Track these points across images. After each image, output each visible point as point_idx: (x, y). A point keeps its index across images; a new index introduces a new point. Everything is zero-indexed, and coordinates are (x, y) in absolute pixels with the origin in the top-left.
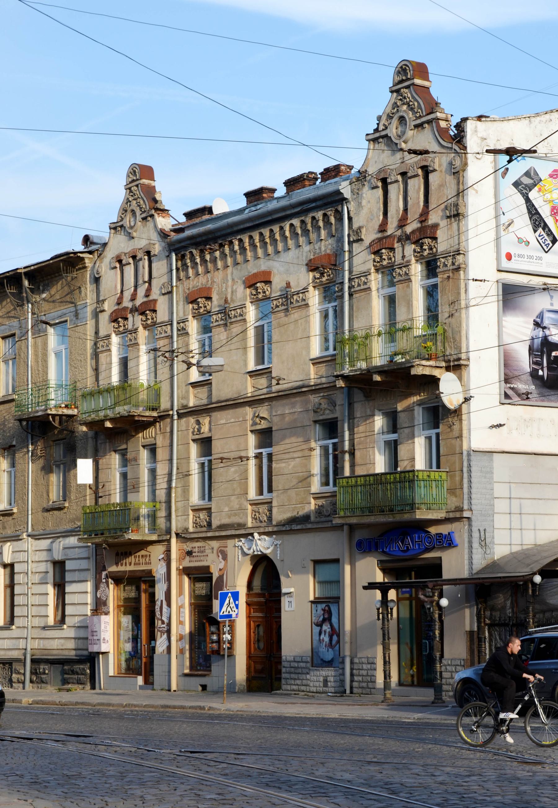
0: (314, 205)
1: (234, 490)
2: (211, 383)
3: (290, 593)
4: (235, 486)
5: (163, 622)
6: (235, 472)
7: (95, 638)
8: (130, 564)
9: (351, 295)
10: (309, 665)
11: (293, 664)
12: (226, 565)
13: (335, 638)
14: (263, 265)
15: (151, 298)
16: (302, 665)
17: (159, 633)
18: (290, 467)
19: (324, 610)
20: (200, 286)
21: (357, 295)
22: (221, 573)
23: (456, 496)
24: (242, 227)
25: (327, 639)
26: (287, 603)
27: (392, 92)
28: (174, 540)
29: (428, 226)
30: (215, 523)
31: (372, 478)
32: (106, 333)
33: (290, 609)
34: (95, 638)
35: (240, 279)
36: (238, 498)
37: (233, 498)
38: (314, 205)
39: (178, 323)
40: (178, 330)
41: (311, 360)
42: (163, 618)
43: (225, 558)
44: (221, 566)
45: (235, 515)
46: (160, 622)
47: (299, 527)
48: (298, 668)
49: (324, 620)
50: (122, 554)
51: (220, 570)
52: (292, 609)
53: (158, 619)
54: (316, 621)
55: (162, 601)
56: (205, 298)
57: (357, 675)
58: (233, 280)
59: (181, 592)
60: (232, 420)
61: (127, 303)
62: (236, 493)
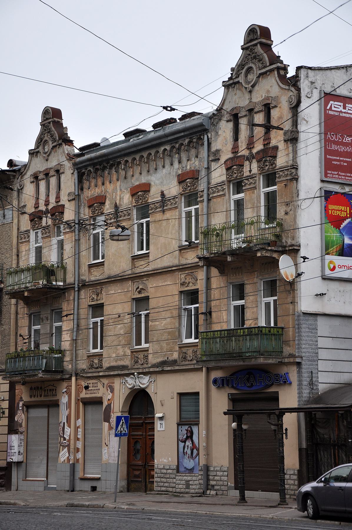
0: (183, 134)
5: (65, 439)
6: (121, 329)
7: (13, 451)
8: (41, 396)
13: (195, 451)
14: (144, 179)
15: (60, 204)
17: (61, 447)
18: (162, 325)
19: (187, 430)
20: (96, 195)
21: (215, 200)
22: (109, 402)
23: (290, 346)
24: (128, 151)
25: (189, 452)
26: (159, 425)
27: (243, 49)
28: (74, 379)
29: (270, 148)
31: (226, 332)
32: (25, 229)
33: (161, 429)
34: (13, 451)
35: (126, 189)
36: (123, 347)
37: (119, 347)
38: (183, 134)
42: (65, 436)
43: (112, 391)
44: (110, 397)
45: (121, 360)
46: (62, 439)
47: (169, 368)
48: (166, 473)
49: (187, 438)
50: (35, 389)
51: (109, 400)
52: (163, 429)
53: (61, 437)
54: (181, 439)
55: (64, 423)
56: (99, 203)
58: (121, 190)
59: (77, 417)
60: (119, 291)
61: (42, 208)
62: (121, 343)
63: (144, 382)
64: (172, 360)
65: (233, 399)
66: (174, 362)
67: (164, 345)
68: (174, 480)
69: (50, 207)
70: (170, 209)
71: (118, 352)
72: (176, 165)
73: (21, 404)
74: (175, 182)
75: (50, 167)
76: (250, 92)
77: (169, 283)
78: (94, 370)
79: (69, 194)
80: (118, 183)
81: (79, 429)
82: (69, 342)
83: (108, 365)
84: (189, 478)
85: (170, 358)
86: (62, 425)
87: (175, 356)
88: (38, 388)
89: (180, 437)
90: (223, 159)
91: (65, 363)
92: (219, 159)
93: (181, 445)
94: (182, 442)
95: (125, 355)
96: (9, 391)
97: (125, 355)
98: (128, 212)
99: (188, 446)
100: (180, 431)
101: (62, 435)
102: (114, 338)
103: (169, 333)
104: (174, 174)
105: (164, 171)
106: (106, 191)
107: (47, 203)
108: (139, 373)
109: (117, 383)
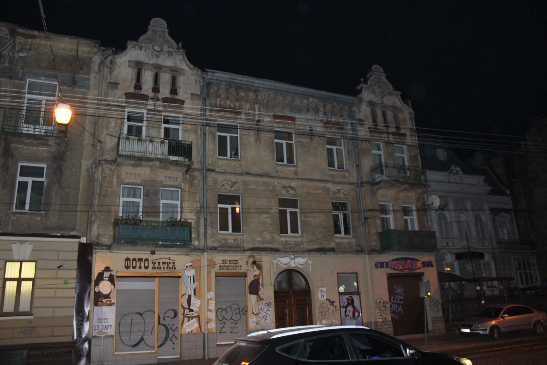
4: (267, 226)
5: (191, 310)
12: (261, 273)
13: (357, 314)
15: (177, 97)
17: (186, 319)
18: (317, 221)
19: (348, 299)
22: (256, 278)
25: (351, 314)
33: (323, 299)
37: (265, 233)
42: (191, 308)
43: (260, 268)
44: (257, 272)
45: (268, 243)
46: (187, 311)
49: (348, 304)
51: (255, 276)
53: (184, 308)
55: (190, 296)
65: (390, 277)
69: (161, 96)
73: (107, 274)
75: (163, 64)
81: (210, 302)
85: (327, 246)
86: (186, 297)
88: (140, 260)
89: (342, 305)
93: (343, 310)
94: (343, 307)
96: (79, 260)
101: (186, 305)
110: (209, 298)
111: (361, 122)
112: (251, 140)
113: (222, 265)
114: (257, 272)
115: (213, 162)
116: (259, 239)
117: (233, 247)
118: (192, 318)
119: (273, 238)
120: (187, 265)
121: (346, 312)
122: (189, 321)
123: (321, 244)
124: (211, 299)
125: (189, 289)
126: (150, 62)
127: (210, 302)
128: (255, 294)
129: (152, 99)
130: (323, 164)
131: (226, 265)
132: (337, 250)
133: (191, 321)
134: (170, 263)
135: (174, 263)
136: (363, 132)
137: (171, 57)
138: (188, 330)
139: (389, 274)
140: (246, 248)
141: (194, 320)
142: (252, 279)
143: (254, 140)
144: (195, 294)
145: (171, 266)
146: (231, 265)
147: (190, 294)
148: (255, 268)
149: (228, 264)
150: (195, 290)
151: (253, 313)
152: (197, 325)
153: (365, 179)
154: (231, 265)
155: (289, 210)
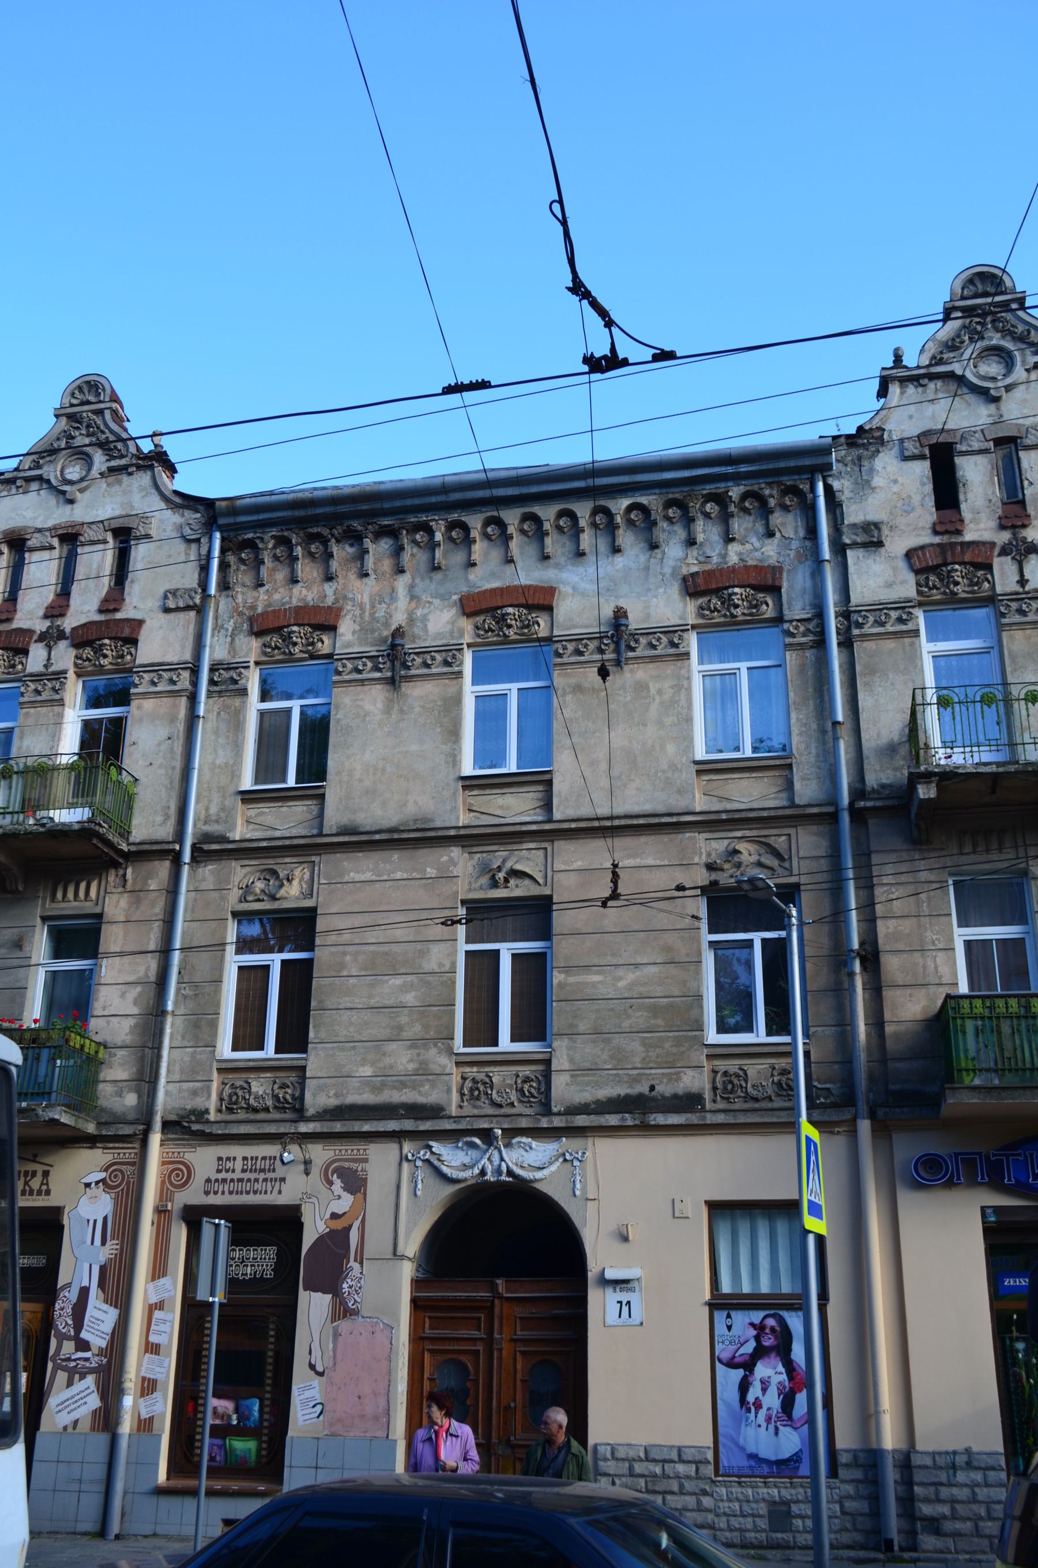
1: (400, 1028)
2: (323, 796)
3: (626, 1281)
4: (404, 1019)
5: (83, 1345)
6: (404, 989)
9: (847, 643)
10: (709, 1470)
11: (639, 1468)
12: (360, 1209)
15: (119, 616)
16: (681, 1468)
17: (62, 1376)
18: (621, 984)
19: (760, 1328)
20: (295, 602)
21: (871, 645)
22: (338, 1225)
25: (772, 1401)
26: (613, 1309)
28: (155, 1139)
30: (315, 1100)
35: (443, 597)
36: (410, 1047)
37: (393, 1046)
38: (730, 469)
39: (213, 670)
40: (212, 682)
41: (697, 763)
42: (84, 1335)
43: (355, 1184)
45: (403, 1085)
46: (68, 1347)
49: (760, 1353)
51: (334, 1216)
54: (726, 1356)
55: (84, 1292)
56: (309, 625)
57: (927, 1500)
58: (413, 597)
59: (159, 1270)
60: (399, 875)
63: (532, 1160)
64: (675, 1096)
66: (690, 1102)
67: (634, 1046)
68: (707, 1502)
69: (69, 623)
70: (653, 659)
71: (388, 1061)
72: (673, 550)
74: (674, 590)
76: (996, 400)
77: (650, 861)
78: (242, 1115)
79: (174, 593)
80: (402, 583)
82: (127, 1024)
83: (333, 1102)
84: (787, 1494)
85: (665, 1089)
86: (73, 1295)
87: (695, 1080)
89: (724, 1351)
90: (897, 545)
91: (101, 1086)
92: (880, 544)
94: (731, 1364)
95: (423, 1071)
97: (423, 1071)
98: (450, 655)
99: (765, 1385)
100: (720, 1328)
102: (366, 1016)
103: (655, 1011)
104: (667, 570)
105: (619, 560)
106: (341, 597)
107: (57, 609)
108: (511, 1133)
109: (380, 1162)
110: (153, 1299)
111: (872, 538)
112: (368, 707)
113: (214, 1176)
114: (345, 1203)
115: (223, 809)
116: (367, 1071)
117: (267, 1110)
118: (82, 1377)
119: (423, 1063)
120: (87, 1180)
121: (744, 1387)
122: (70, 1384)
123: (636, 1080)
124: (160, 1306)
125: (86, 1266)
126: (50, 524)
127: (157, 1314)
128: (324, 1292)
129: (43, 637)
130: (671, 748)
131: (229, 1176)
132: (708, 1105)
133: (79, 1386)
134: (34, 1174)
135: (46, 1174)
136: (878, 578)
137: (116, 488)
138: (65, 1419)
139: (997, 1210)
140: (311, 1111)
141: (90, 1380)
142: (322, 1228)
143: (380, 705)
144: (102, 1285)
145: (35, 1183)
146: (246, 1176)
147: (85, 1283)
148: (338, 1184)
149: (238, 1175)
150: (103, 1269)
151: (312, 1367)
152: (94, 1402)
153: (872, 780)
154: (246, 1176)
155: (506, 951)
